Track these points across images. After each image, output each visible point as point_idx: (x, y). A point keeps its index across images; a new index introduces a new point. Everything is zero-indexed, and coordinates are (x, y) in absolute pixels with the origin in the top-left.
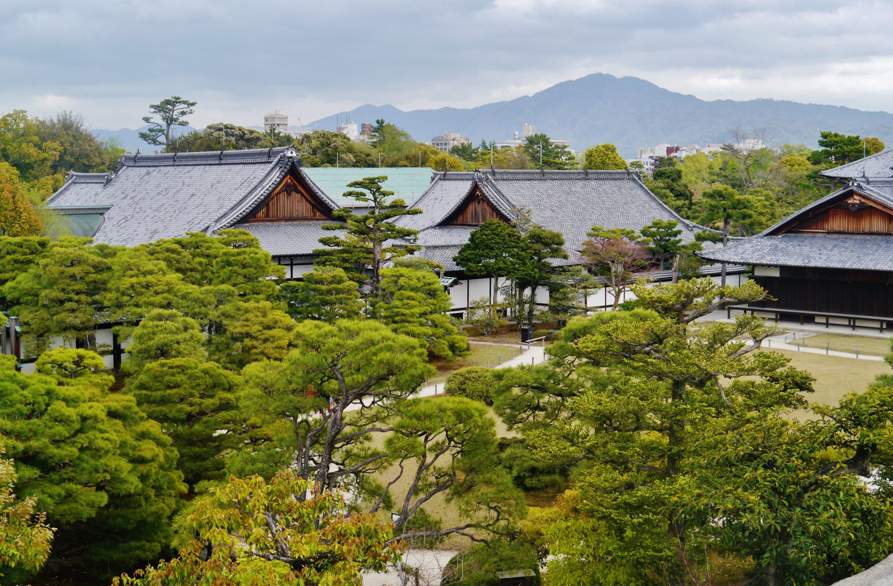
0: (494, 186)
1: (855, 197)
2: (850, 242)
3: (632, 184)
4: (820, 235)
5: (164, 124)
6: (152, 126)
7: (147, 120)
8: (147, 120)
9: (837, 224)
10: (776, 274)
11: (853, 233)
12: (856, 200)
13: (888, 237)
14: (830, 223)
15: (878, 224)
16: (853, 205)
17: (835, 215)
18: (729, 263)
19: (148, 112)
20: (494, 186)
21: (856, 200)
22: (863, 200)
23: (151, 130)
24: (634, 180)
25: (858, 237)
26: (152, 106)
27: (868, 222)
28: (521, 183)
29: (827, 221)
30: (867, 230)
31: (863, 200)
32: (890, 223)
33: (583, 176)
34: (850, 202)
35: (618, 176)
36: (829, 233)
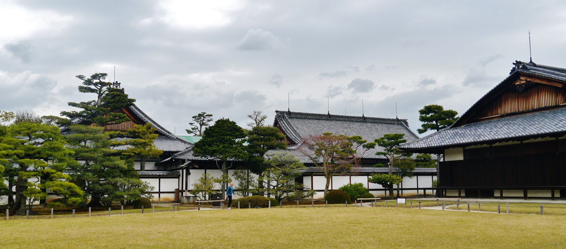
0: (286, 121)
1: (522, 78)
2: (519, 120)
3: (400, 127)
4: (495, 120)
5: (199, 126)
6: (193, 127)
7: (191, 124)
8: (191, 124)
9: (509, 107)
10: (460, 158)
11: (523, 113)
12: (523, 81)
13: (556, 110)
14: (503, 108)
15: (546, 100)
16: (520, 85)
17: (506, 100)
18: (538, 213)
19: (192, 120)
20: (286, 121)
21: (523, 81)
22: (529, 80)
23: (193, 129)
24: (402, 125)
25: (528, 115)
26: (193, 117)
27: (536, 98)
28: (311, 121)
29: (500, 107)
30: (536, 107)
31: (529, 80)
32: (557, 96)
33: (363, 120)
34: (517, 84)
35: (389, 122)
36: (502, 116)
